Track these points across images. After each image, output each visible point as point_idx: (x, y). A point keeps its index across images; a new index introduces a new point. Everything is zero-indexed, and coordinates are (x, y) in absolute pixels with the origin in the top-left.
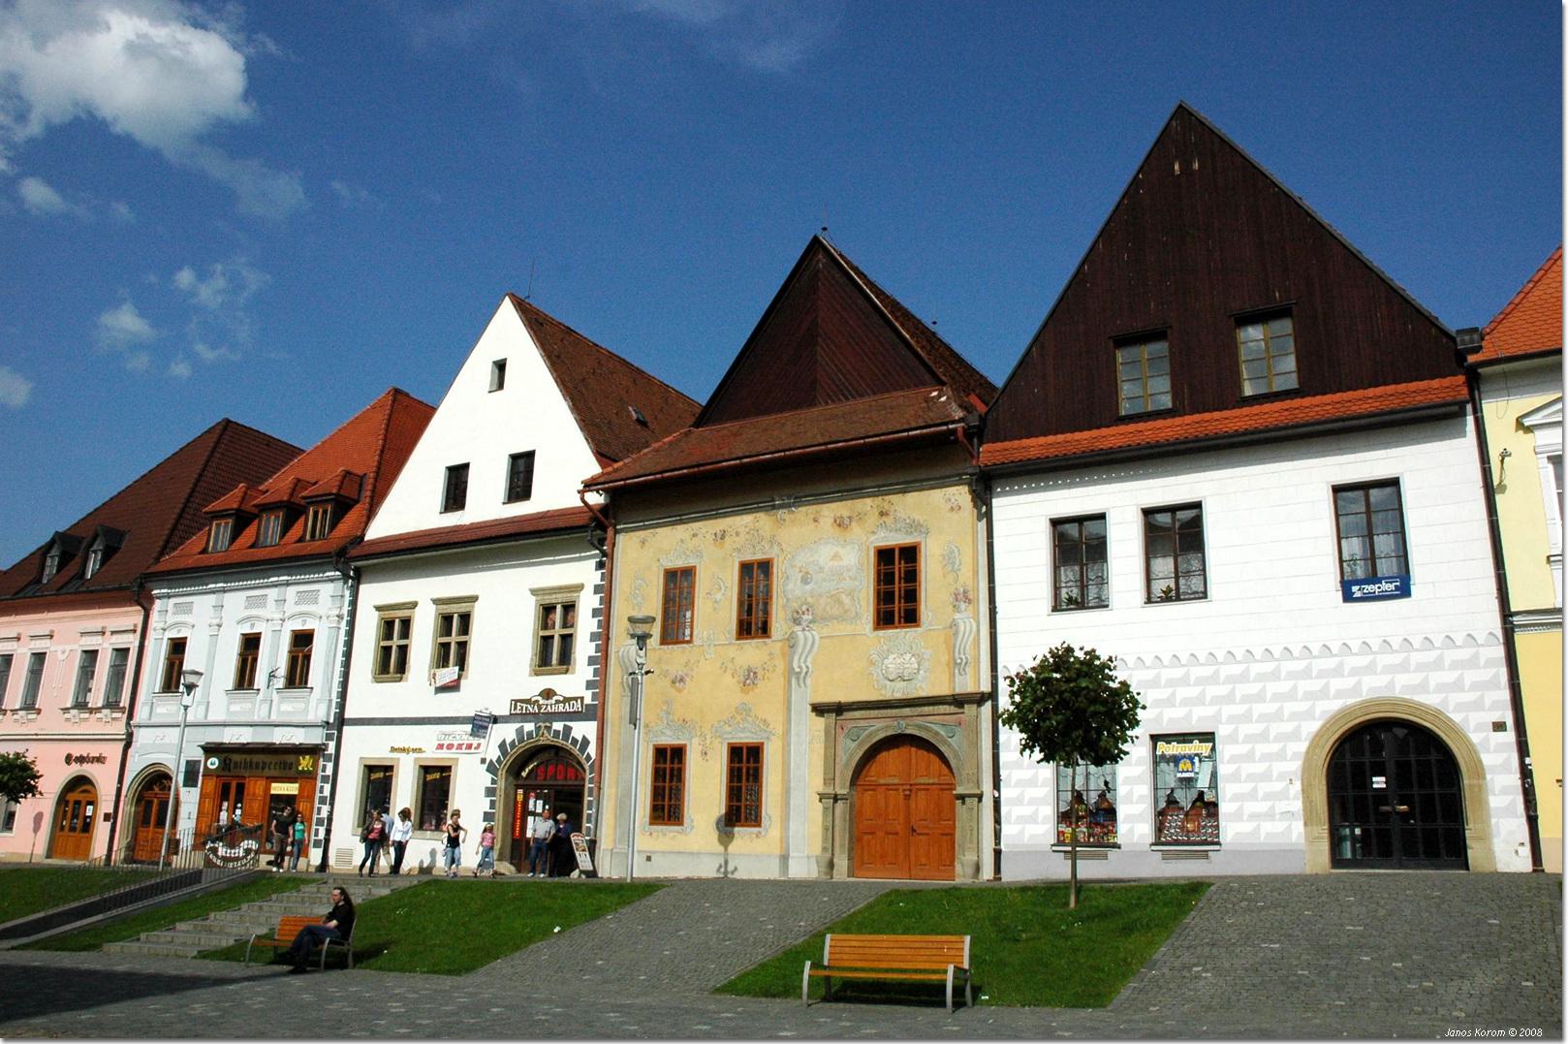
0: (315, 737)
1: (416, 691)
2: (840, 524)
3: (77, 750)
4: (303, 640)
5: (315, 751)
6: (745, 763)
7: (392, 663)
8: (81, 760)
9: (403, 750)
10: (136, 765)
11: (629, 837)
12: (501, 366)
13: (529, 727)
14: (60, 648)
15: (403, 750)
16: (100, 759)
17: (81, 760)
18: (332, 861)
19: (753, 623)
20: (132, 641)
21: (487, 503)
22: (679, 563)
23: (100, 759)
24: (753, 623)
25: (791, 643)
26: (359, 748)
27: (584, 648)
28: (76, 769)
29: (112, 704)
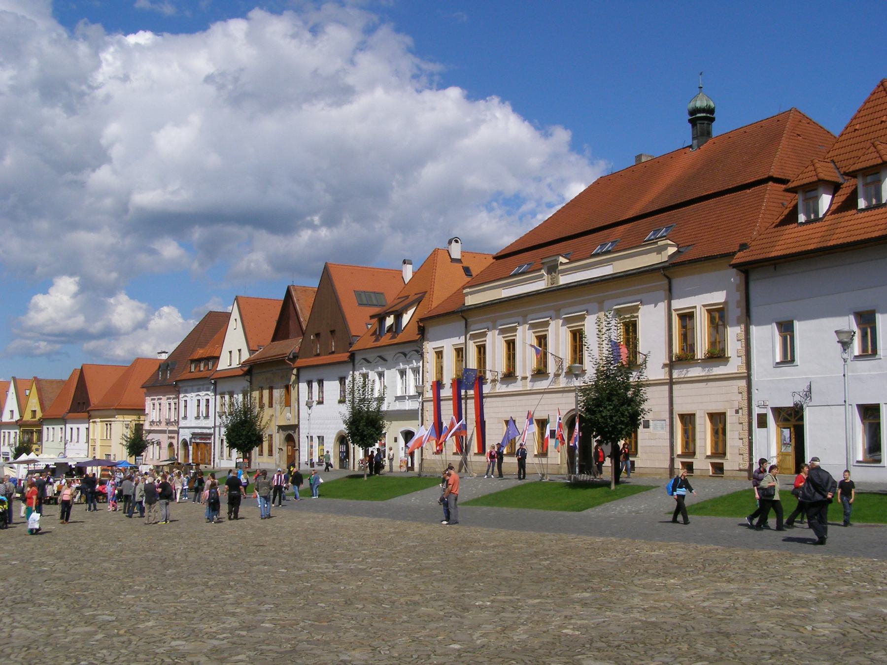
0: (212, 431)
4: (208, 400)
5: (211, 434)
10: (181, 439)
16: (173, 438)
18: (215, 466)
21: (234, 365)
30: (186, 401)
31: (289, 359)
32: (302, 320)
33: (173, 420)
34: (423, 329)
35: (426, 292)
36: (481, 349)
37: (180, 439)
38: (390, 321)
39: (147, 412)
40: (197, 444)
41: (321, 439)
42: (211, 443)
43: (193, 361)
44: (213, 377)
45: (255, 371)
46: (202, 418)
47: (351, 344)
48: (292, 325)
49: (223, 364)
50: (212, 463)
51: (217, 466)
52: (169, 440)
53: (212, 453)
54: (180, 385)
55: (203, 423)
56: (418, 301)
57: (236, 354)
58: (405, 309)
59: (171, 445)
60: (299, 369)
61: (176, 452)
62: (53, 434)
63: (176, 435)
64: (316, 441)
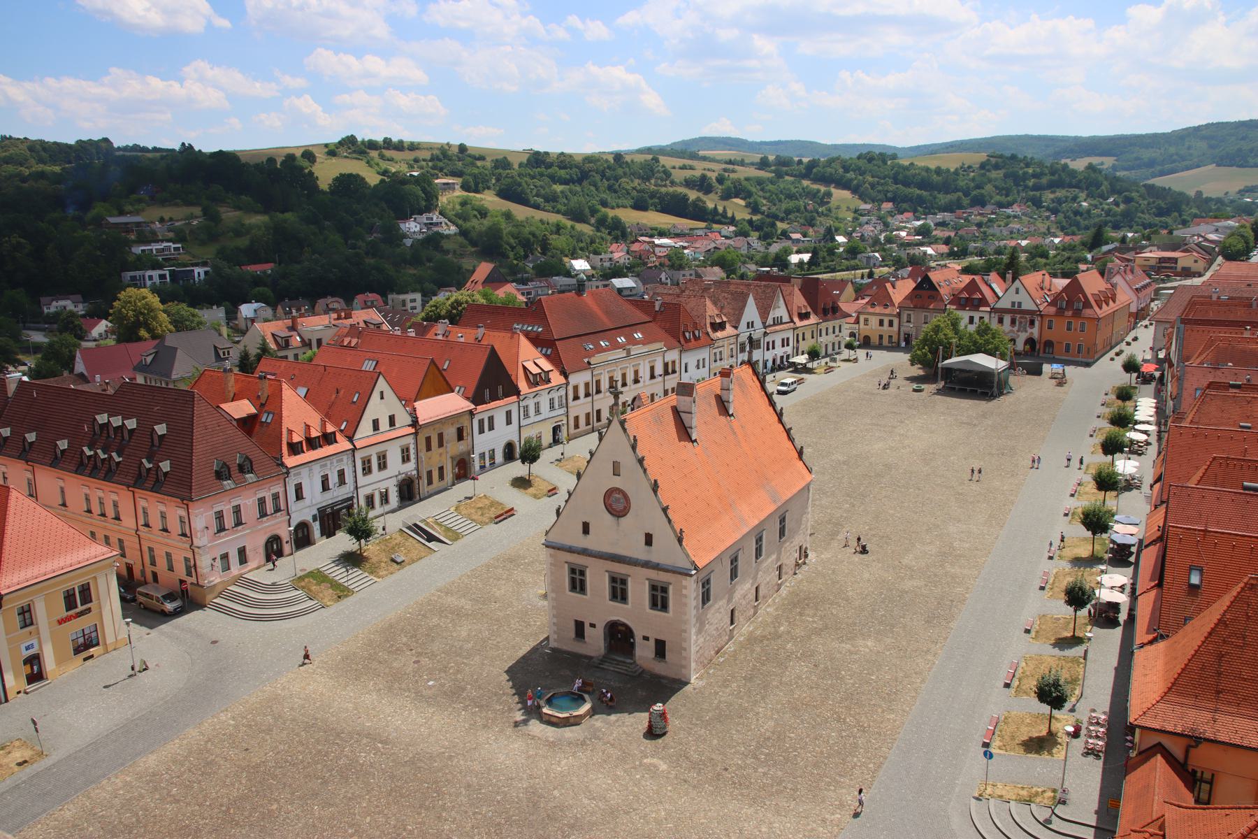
0: (350, 495)
1: (376, 474)
2: (452, 424)
4: (341, 474)
6: (441, 469)
7: (367, 470)
10: (294, 523)
12: (382, 393)
14: (247, 501)
19: (441, 444)
20: (280, 489)
22: (428, 435)
24: (441, 444)
25: (446, 447)
26: (363, 493)
27: (412, 456)
29: (277, 510)
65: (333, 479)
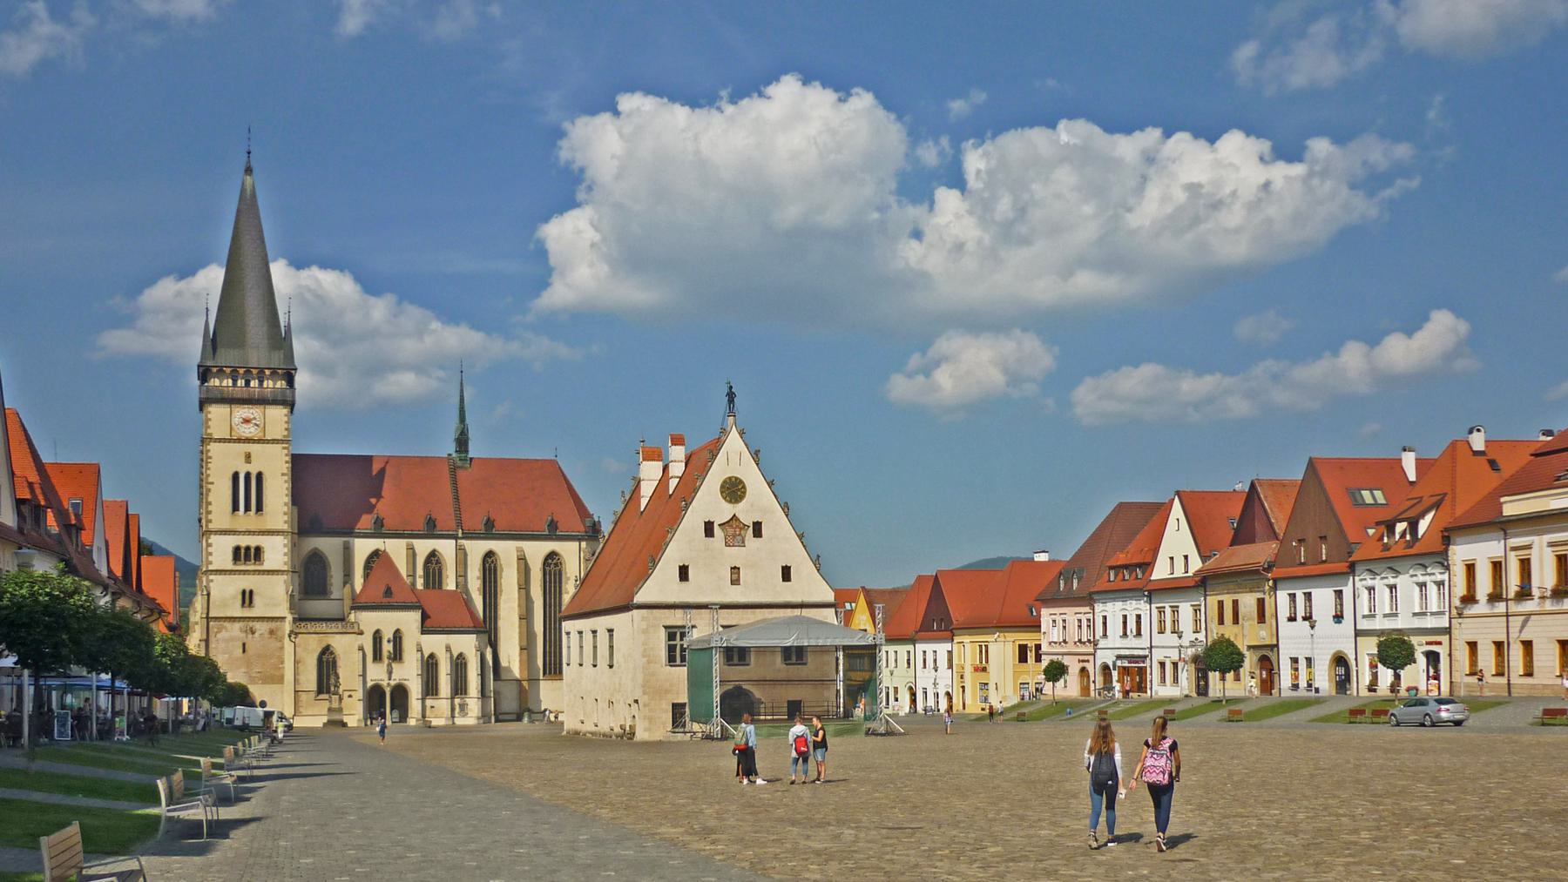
0: (1147, 652)
1: (1169, 638)
3: (1082, 658)
4: (1139, 617)
5: (1146, 657)
8: (1083, 661)
9: (1166, 657)
10: (1099, 663)
11: (1215, 685)
13: (1194, 649)
15: (1166, 657)
16: (1088, 661)
17: (1083, 661)
18: (1153, 694)
19: (1236, 620)
20: (1091, 616)
23: (1088, 661)
24: (1236, 620)
28: (1082, 665)
30: (1105, 617)
31: (1264, 570)
32: (1273, 521)
33: (1086, 640)
34: (1447, 537)
35: (1445, 494)
36: (1525, 565)
37: (1099, 663)
38: (1401, 527)
39: (1043, 629)
40: (1124, 668)
41: (1309, 660)
42: (1146, 667)
43: (1111, 568)
44: (1148, 588)
45: (1209, 582)
46: (1130, 637)
47: (1350, 554)
48: (1259, 526)
49: (1160, 572)
50: (1149, 691)
51: (1156, 694)
52: (1081, 664)
53: (1148, 680)
54: (1095, 597)
55: (1132, 642)
56: (1437, 505)
57: (1179, 564)
58: (1423, 515)
59: (1083, 670)
60: (1275, 581)
61: (1092, 679)
62: (896, 660)
63: (1091, 658)
64: (1302, 664)
65: (1132, 624)
